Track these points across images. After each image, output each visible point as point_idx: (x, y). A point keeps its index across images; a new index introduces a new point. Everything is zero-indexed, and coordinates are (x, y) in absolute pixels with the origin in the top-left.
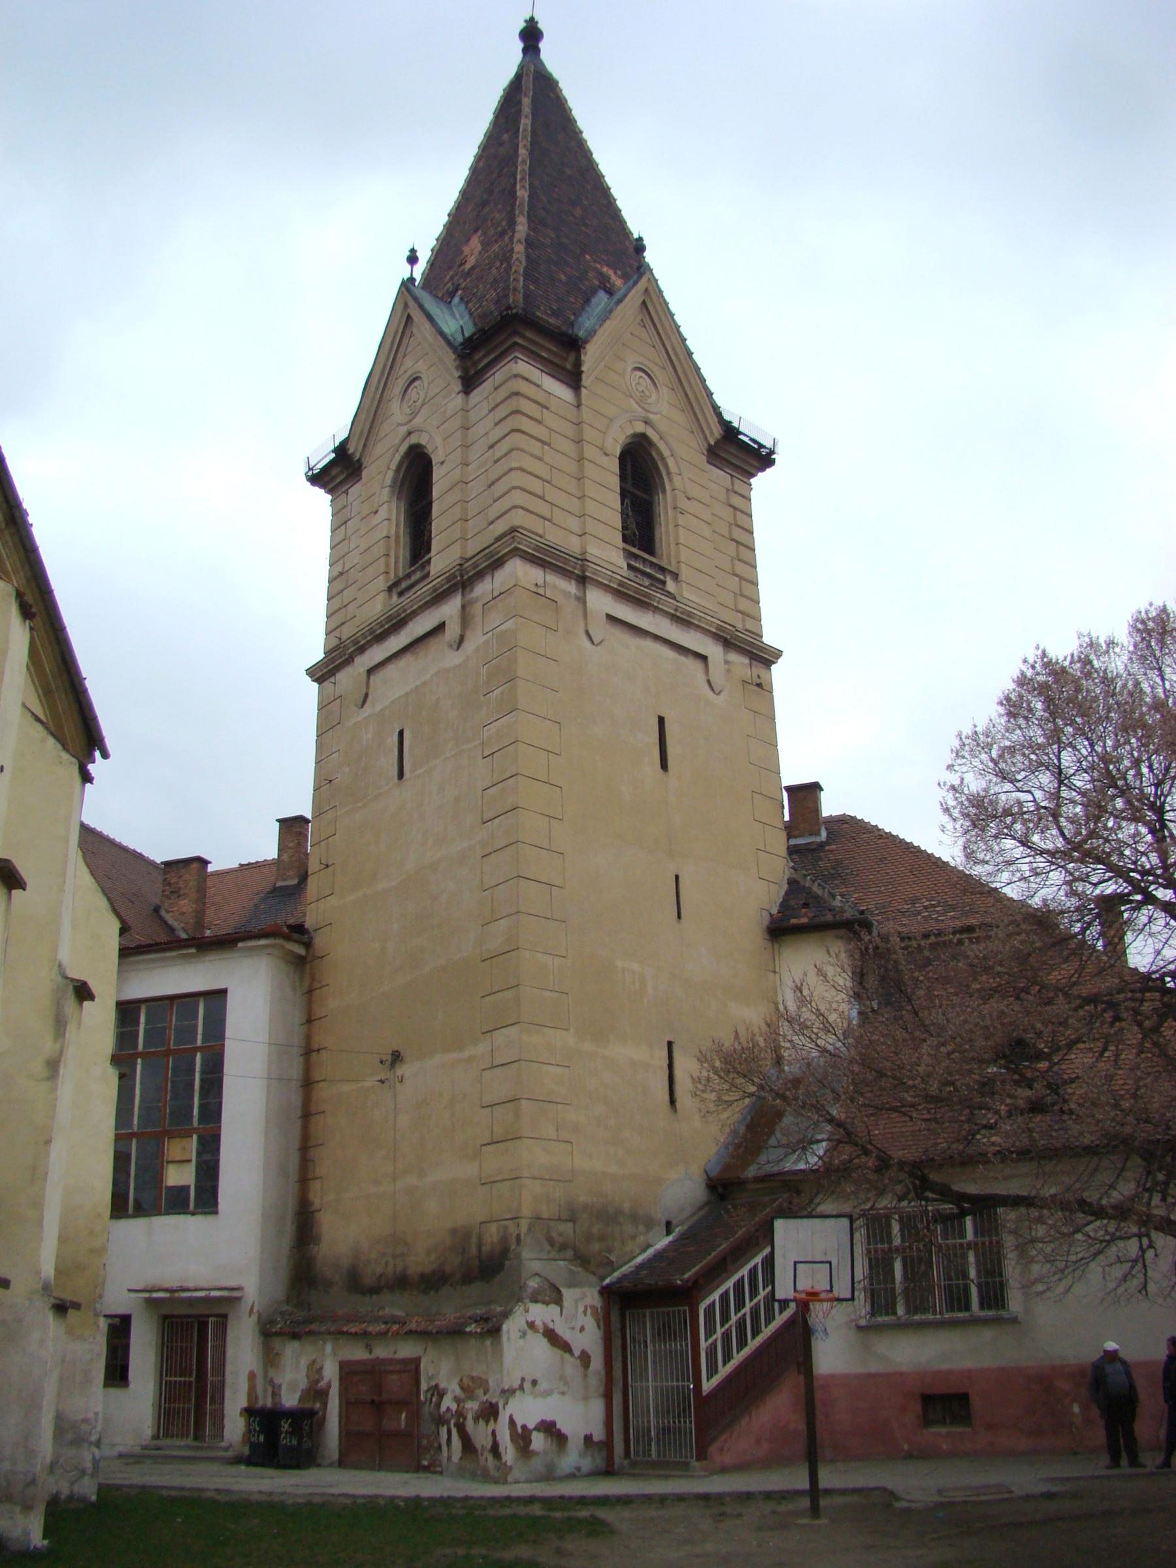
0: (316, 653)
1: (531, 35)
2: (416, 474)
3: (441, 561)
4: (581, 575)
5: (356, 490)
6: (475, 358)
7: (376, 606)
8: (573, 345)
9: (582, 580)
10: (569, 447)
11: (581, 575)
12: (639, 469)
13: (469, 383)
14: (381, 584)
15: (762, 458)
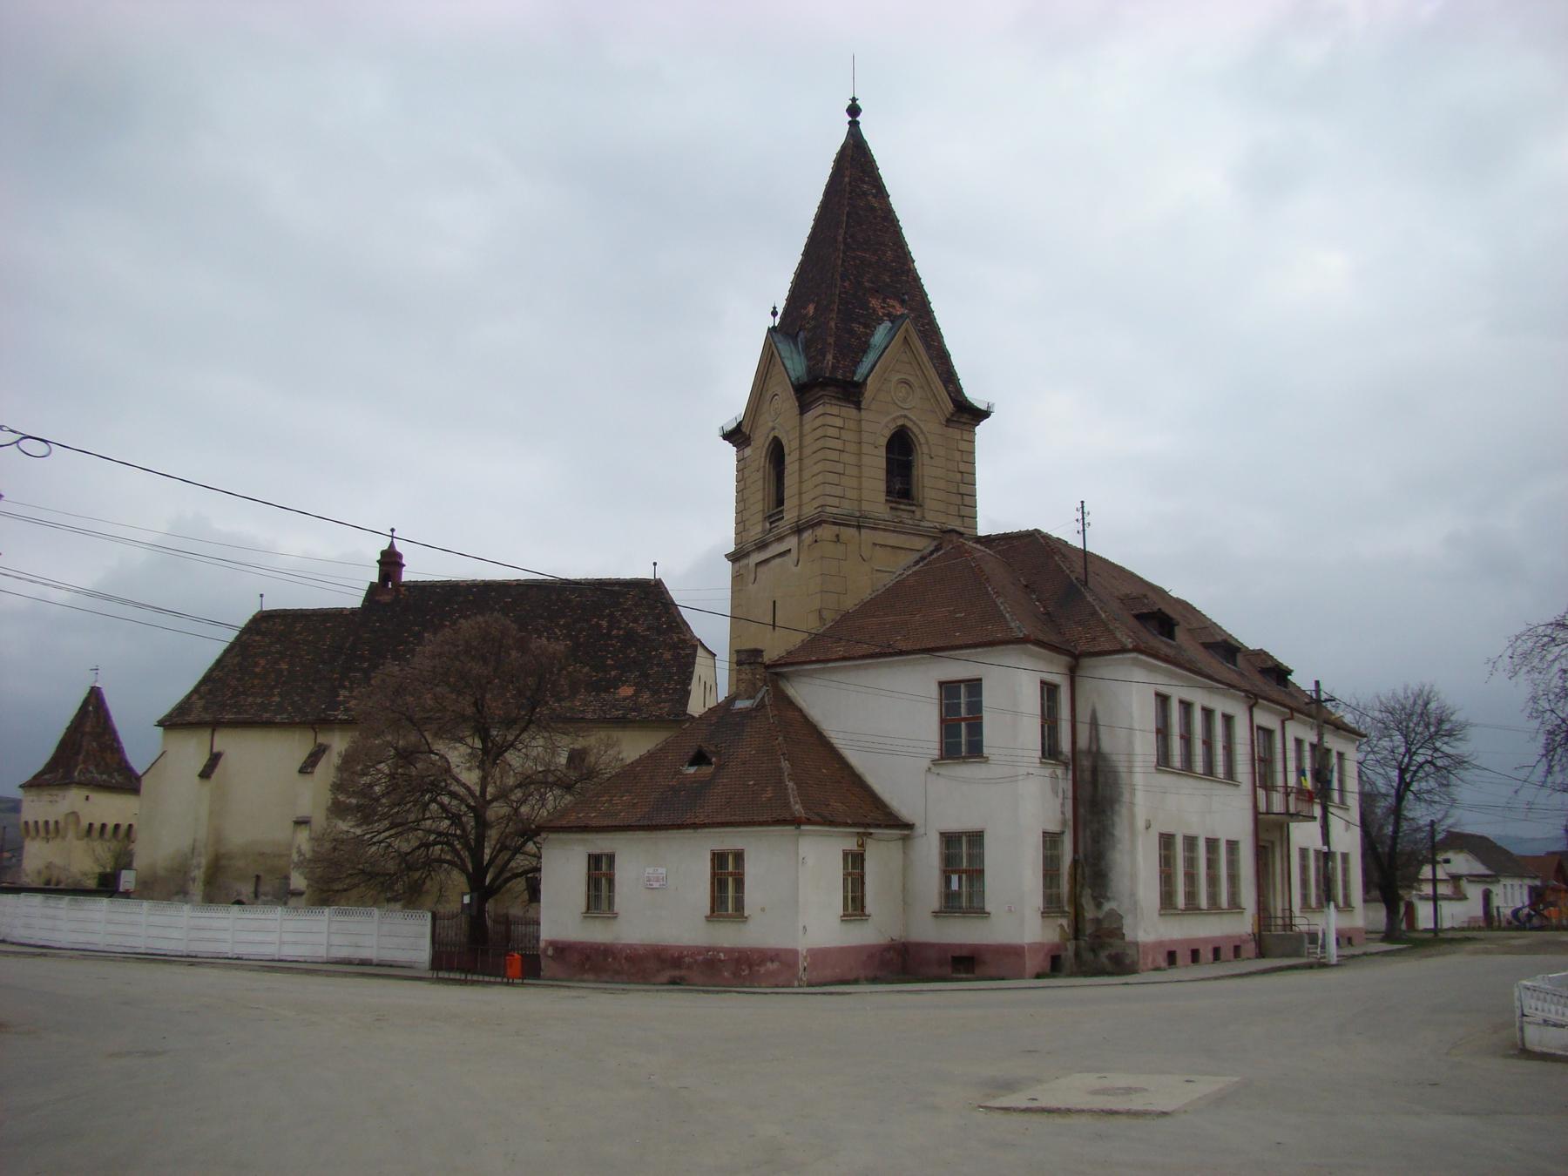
0: (732, 548)
1: (854, 110)
2: (777, 453)
3: (790, 515)
4: (859, 522)
5: (748, 451)
6: (806, 392)
7: (756, 531)
8: (860, 386)
9: (859, 527)
10: (852, 447)
11: (859, 522)
12: (901, 447)
13: (803, 408)
14: (760, 517)
15: (982, 415)
